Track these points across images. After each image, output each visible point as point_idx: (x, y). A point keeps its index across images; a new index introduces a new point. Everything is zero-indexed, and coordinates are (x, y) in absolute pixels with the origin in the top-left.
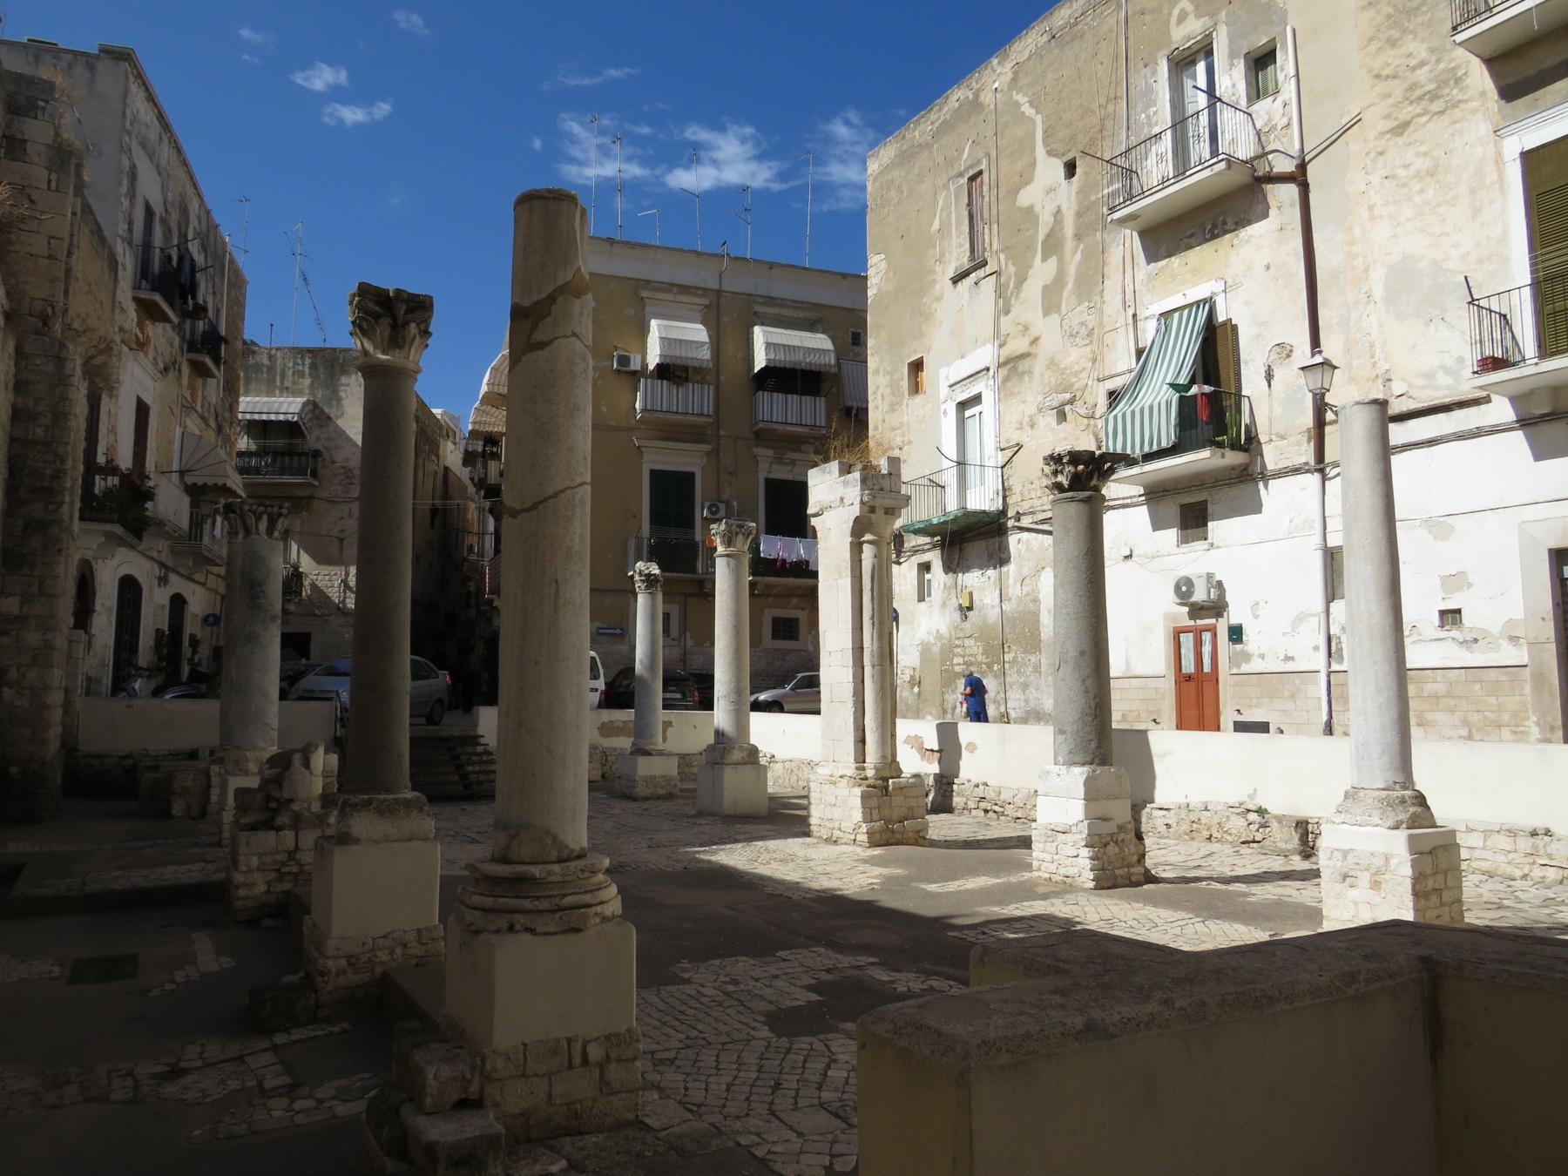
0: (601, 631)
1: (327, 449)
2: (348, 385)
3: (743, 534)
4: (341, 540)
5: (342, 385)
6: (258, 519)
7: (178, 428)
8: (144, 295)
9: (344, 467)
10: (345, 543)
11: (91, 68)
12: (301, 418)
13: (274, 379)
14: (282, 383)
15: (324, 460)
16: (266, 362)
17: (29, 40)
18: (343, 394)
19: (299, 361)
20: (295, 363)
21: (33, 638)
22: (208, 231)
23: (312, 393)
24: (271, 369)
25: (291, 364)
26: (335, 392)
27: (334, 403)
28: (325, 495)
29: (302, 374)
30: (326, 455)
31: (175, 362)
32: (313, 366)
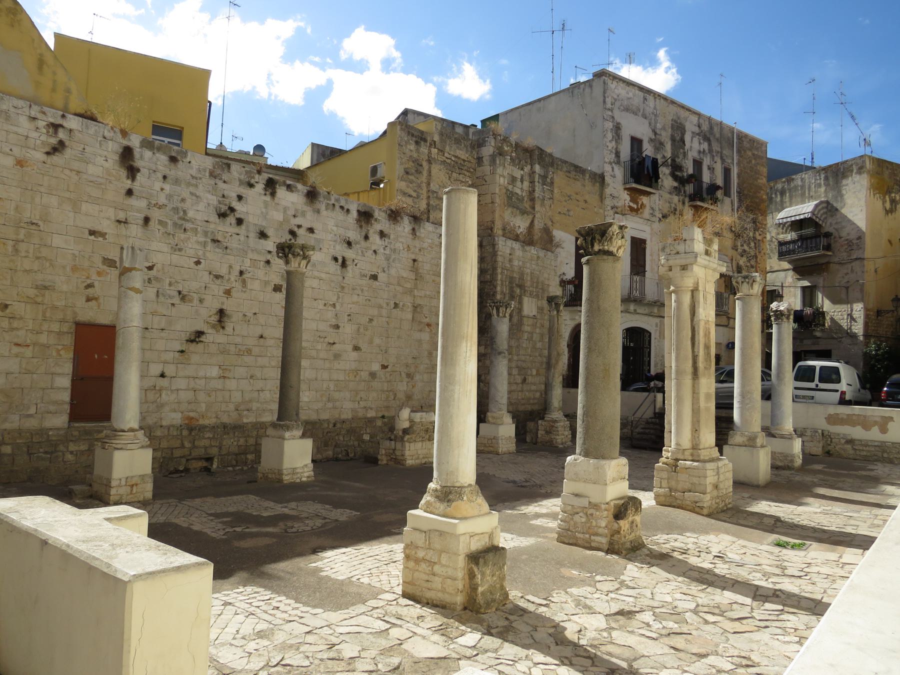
1: (837, 230)
2: (847, 185)
3: (748, 283)
4: (847, 288)
5: (844, 185)
6: (493, 309)
8: (628, 186)
9: (847, 240)
10: (850, 289)
11: (591, 86)
12: (814, 214)
13: (805, 192)
14: (809, 194)
15: (835, 238)
16: (800, 183)
18: (844, 192)
19: (818, 178)
20: (816, 180)
22: (711, 128)
23: (826, 196)
24: (803, 187)
25: (813, 181)
27: (839, 198)
28: (836, 260)
29: (820, 186)
30: (835, 234)
32: (826, 178)
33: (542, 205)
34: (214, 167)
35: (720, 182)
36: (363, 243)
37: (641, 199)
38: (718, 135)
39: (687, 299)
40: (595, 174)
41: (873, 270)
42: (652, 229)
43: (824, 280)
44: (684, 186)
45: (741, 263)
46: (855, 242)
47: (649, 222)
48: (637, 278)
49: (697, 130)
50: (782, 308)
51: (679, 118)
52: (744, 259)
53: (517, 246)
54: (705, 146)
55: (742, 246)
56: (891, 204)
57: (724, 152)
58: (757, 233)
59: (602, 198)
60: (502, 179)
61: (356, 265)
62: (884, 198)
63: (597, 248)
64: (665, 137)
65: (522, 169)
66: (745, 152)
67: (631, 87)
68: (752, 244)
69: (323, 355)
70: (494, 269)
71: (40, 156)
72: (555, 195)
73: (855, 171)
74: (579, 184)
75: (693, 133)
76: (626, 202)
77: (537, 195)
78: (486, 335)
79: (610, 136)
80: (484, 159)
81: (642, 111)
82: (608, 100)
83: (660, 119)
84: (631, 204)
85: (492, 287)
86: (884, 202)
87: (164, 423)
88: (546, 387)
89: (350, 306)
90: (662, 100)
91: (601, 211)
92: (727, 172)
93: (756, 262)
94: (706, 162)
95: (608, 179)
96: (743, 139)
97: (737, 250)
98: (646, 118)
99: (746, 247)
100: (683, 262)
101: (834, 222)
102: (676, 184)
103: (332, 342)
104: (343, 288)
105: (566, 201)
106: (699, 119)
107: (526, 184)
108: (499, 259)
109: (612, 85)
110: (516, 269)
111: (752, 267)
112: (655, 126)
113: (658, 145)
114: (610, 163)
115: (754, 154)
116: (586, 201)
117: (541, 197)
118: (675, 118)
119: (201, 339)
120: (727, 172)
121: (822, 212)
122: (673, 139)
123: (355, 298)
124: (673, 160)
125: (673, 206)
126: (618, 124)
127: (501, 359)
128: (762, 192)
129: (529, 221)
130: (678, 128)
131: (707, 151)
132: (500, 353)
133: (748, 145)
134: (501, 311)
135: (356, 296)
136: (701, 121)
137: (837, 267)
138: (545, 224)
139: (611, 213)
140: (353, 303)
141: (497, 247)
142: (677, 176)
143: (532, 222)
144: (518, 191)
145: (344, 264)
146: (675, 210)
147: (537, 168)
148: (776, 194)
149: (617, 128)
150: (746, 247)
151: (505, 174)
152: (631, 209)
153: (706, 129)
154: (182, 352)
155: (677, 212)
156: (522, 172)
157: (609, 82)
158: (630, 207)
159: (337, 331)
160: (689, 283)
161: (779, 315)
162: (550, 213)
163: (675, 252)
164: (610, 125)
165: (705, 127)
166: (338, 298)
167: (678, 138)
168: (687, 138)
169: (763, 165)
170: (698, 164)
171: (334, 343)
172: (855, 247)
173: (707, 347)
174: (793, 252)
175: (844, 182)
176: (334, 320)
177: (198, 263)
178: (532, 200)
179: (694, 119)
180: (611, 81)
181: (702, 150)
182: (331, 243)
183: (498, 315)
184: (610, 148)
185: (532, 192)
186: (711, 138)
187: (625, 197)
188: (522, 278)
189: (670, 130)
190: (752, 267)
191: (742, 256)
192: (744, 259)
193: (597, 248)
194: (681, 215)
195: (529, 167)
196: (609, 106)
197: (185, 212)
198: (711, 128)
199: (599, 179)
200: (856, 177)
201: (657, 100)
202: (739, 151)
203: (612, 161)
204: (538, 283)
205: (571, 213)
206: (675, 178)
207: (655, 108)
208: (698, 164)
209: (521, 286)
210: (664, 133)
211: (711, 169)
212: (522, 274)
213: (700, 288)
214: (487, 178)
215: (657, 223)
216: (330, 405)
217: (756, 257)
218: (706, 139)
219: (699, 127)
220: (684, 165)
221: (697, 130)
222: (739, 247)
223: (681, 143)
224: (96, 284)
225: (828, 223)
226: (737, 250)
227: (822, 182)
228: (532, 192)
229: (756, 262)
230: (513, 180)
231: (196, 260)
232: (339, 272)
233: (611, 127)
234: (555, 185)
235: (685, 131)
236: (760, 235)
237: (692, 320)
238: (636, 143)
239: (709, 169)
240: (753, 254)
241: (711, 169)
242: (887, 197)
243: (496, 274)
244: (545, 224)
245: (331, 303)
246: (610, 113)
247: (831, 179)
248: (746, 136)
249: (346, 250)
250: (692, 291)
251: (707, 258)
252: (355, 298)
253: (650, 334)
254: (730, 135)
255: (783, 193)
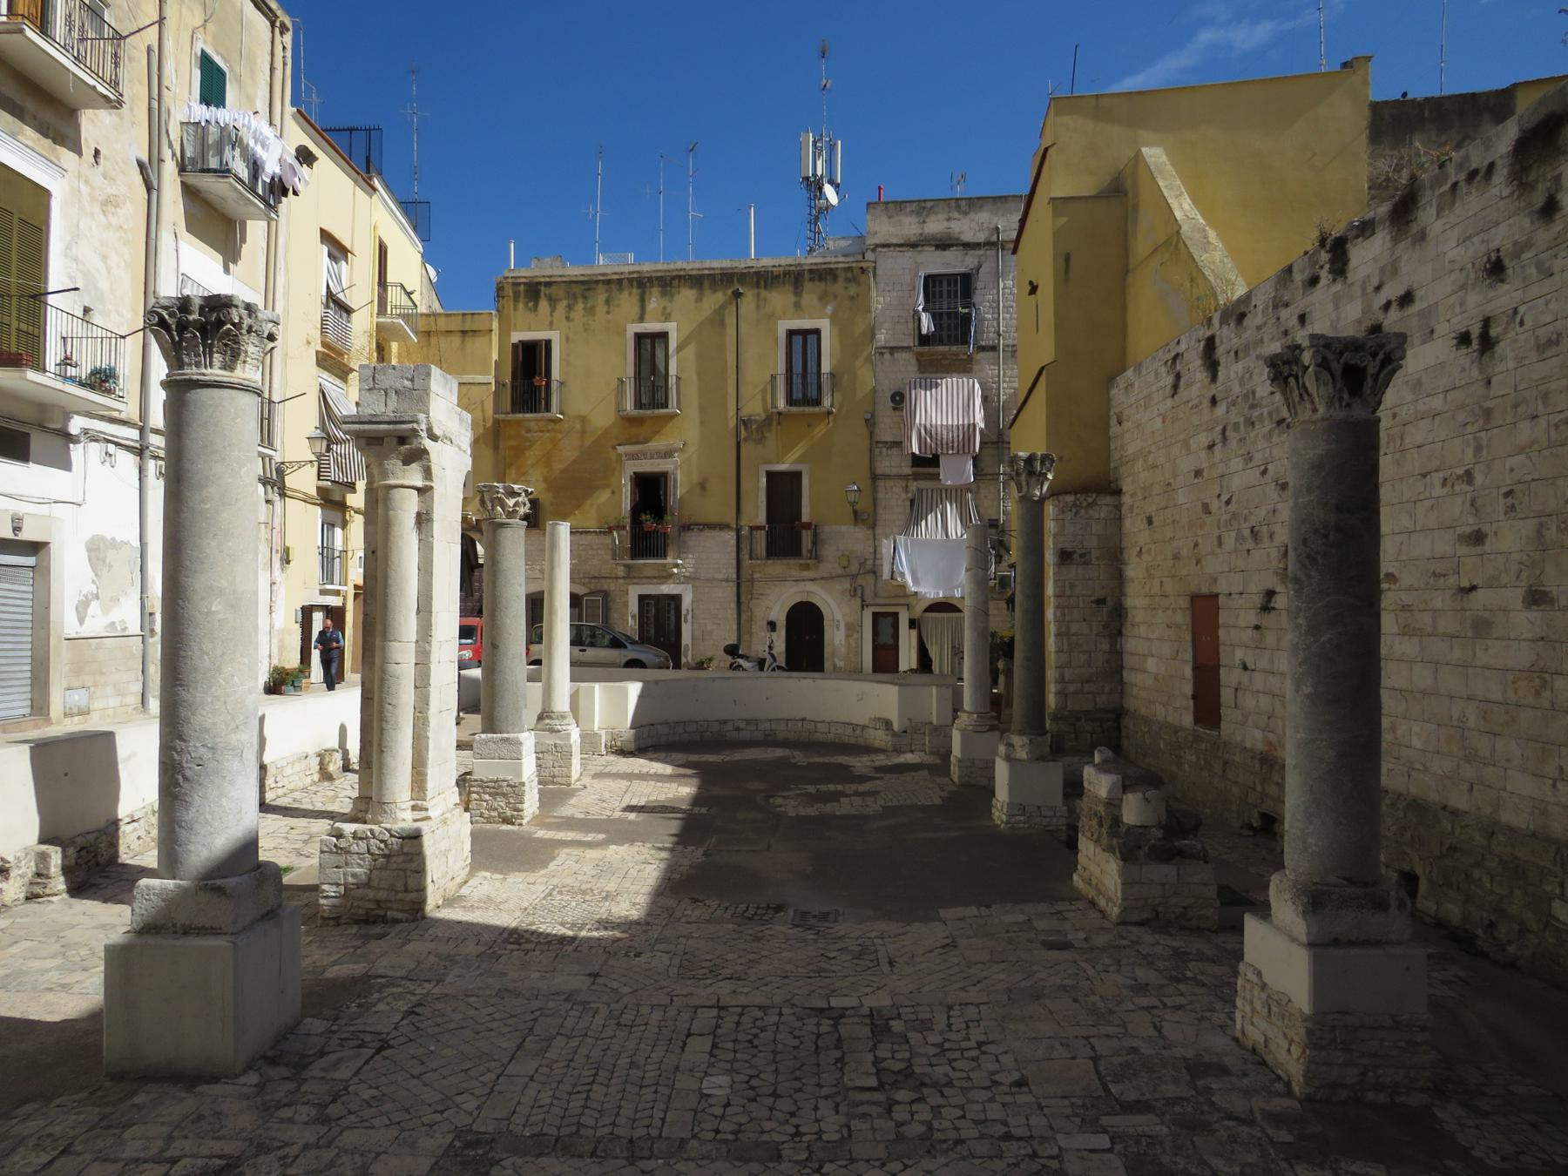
34: (1277, 290)
36: (1543, 236)
61: (1522, 323)
69: (1446, 624)
71: (1169, 402)
87: (1248, 745)
89: (1510, 462)
103: (1465, 584)
104: (1488, 413)
119: (1272, 605)
123: (1525, 432)
135: (1528, 423)
140: (1521, 450)
145: (1487, 343)
154: (1257, 627)
159: (1478, 550)
166: (1478, 449)
171: (1473, 588)
176: (1471, 520)
177: (1264, 472)
182: (1453, 298)
197: (1254, 393)
216: (1469, 772)
224: (1200, 541)
231: (1263, 467)
232: (1475, 374)
245: (1460, 471)
249: (1491, 294)
252: (1525, 432)
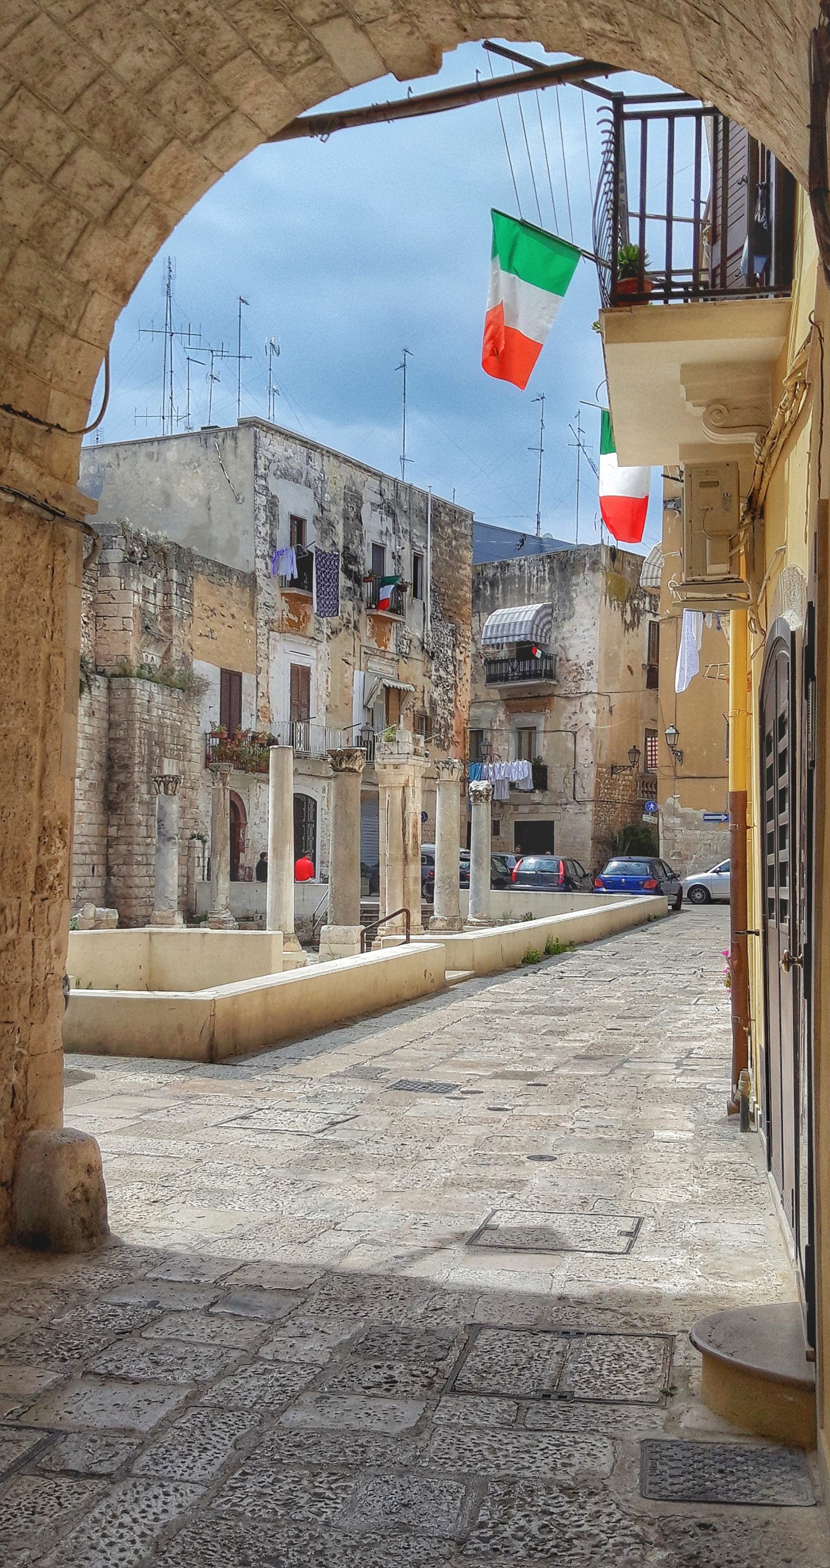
0: (706, 818)
2: (577, 585)
4: (575, 734)
6: (159, 785)
7: (357, 672)
9: (576, 664)
11: (235, 438)
13: (524, 586)
14: (529, 590)
16: (517, 573)
17: (202, 428)
19: (541, 568)
21: (123, 848)
22: (397, 495)
24: (521, 578)
25: (535, 572)
26: (568, 593)
27: (568, 604)
31: (349, 622)
32: (552, 571)
33: (181, 626)
35: (408, 577)
37: (304, 608)
38: (405, 507)
39: (399, 794)
40: (245, 575)
41: (607, 708)
42: (318, 652)
43: (546, 720)
44: (360, 585)
45: (435, 696)
46: (585, 668)
47: (316, 642)
48: (300, 726)
49: (377, 499)
50: (481, 788)
51: (354, 484)
52: (440, 689)
53: (155, 689)
54: (388, 523)
55: (437, 670)
56: (633, 616)
57: (415, 531)
58: (457, 650)
59: (253, 608)
60: (136, 596)
62: (624, 606)
63: (344, 766)
64: (335, 513)
65: (156, 577)
66: (442, 528)
67: (290, 440)
68: (451, 668)
70: (131, 722)
72: (194, 610)
73: (588, 566)
74: (224, 590)
75: (372, 504)
76: (284, 613)
77: (174, 613)
78: (119, 812)
79: (262, 516)
80: (110, 566)
81: (304, 476)
82: (261, 463)
83: (329, 487)
84: (291, 616)
85: (127, 747)
86: (623, 612)
88: (188, 881)
90: (332, 458)
91: (253, 628)
92: (417, 559)
93: (456, 693)
94: (391, 546)
95: (261, 581)
96: (441, 509)
97: (430, 678)
98: (310, 487)
99: (442, 673)
100: (397, 762)
101: (560, 637)
102: (349, 584)
105: (208, 617)
106: (381, 482)
107: (159, 596)
108: (137, 708)
109: (265, 439)
110: (155, 720)
111: (450, 701)
112: (322, 499)
113: (326, 527)
114: (263, 557)
115: (454, 532)
116: (233, 616)
117: (179, 615)
118: (349, 484)
120: (417, 559)
121: (545, 621)
122: (346, 518)
124: (346, 548)
125: (346, 615)
126: (274, 497)
127: (170, 846)
128: (465, 588)
129: (164, 649)
130: (354, 498)
131: (391, 532)
132: (170, 839)
133: (447, 519)
134: (170, 787)
136: (384, 485)
137: (563, 702)
138: (184, 653)
139: (265, 630)
141: (133, 692)
142: (351, 570)
143: (168, 650)
144: (151, 609)
146: (349, 622)
147: (174, 575)
148: (484, 584)
149: (273, 504)
150: (442, 673)
151: (140, 589)
152: (291, 623)
153: (390, 497)
155: (351, 626)
156: (155, 580)
157: (262, 434)
158: (289, 620)
160: (402, 780)
161: (478, 795)
162: (189, 637)
163: (389, 752)
164: (262, 500)
165: (389, 495)
167: (352, 514)
168: (365, 511)
169: (466, 548)
170: (378, 550)
172: (585, 676)
173: (415, 836)
174: (505, 678)
175: (574, 580)
178: (168, 619)
179: (374, 483)
180: (264, 434)
181: (385, 531)
183: (166, 793)
184: (262, 535)
185: (167, 608)
186: (397, 511)
187: (282, 605)
188: (161, 733)
189: (342, 502)
190: (450, 701)
191: (437, 686)
192: (440, 689)
193: (344, 766)
194: (356, 627)
195: (163, 571)
196: (262, 471)
198: (397, 495)
199: (249, 581)
200: (589, 575)
201: (325, 458)
202: (434, 529)
203: (266, 553)
204: (178, 737)
205: (215, 635)
206: (349, 573)
207: (322, 471)
208: (378, 550)
209: (160, 744)
210: (333, 509)
211: (397, 558)
212: (161, 725)
213: (410, 785)
214: (114, 594)
215: (325, 641)
217: (456, 687)
218: (391, 513)
219: (381, 494)
220: (360, 554)
221: (377, 499)
222: (434, 673)
223: (357, 522)
225: (553, 638)
226: (430, 678)
227: (547, 576)
228: (167, 608)
229: (456, 693)
230: (146, 592)
233: (265, 503)
234: (196, 596)
235: (362, 503)
236: (461, 653)
237: (403, 814)
238: (298, 524)
239: (394, 557)
240: (451, 681)
241: (397, 558)
242: (628, 604)
243: (134, 730)
244: (184, 653)
246: (263, 482)
247: (557, 573)
248: (445, 504)
250: (404, 788)
251: (416, 758)
253: (316, 802)
254: (422, 504)
255: (493, 584)
